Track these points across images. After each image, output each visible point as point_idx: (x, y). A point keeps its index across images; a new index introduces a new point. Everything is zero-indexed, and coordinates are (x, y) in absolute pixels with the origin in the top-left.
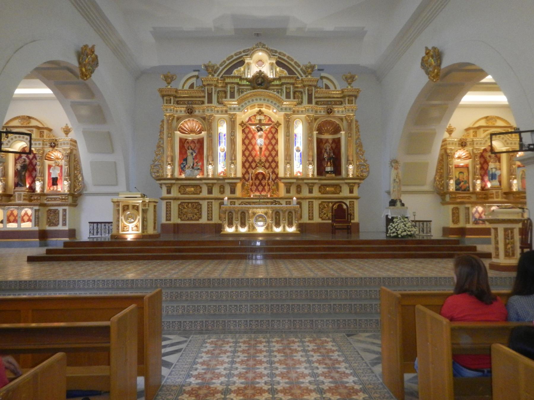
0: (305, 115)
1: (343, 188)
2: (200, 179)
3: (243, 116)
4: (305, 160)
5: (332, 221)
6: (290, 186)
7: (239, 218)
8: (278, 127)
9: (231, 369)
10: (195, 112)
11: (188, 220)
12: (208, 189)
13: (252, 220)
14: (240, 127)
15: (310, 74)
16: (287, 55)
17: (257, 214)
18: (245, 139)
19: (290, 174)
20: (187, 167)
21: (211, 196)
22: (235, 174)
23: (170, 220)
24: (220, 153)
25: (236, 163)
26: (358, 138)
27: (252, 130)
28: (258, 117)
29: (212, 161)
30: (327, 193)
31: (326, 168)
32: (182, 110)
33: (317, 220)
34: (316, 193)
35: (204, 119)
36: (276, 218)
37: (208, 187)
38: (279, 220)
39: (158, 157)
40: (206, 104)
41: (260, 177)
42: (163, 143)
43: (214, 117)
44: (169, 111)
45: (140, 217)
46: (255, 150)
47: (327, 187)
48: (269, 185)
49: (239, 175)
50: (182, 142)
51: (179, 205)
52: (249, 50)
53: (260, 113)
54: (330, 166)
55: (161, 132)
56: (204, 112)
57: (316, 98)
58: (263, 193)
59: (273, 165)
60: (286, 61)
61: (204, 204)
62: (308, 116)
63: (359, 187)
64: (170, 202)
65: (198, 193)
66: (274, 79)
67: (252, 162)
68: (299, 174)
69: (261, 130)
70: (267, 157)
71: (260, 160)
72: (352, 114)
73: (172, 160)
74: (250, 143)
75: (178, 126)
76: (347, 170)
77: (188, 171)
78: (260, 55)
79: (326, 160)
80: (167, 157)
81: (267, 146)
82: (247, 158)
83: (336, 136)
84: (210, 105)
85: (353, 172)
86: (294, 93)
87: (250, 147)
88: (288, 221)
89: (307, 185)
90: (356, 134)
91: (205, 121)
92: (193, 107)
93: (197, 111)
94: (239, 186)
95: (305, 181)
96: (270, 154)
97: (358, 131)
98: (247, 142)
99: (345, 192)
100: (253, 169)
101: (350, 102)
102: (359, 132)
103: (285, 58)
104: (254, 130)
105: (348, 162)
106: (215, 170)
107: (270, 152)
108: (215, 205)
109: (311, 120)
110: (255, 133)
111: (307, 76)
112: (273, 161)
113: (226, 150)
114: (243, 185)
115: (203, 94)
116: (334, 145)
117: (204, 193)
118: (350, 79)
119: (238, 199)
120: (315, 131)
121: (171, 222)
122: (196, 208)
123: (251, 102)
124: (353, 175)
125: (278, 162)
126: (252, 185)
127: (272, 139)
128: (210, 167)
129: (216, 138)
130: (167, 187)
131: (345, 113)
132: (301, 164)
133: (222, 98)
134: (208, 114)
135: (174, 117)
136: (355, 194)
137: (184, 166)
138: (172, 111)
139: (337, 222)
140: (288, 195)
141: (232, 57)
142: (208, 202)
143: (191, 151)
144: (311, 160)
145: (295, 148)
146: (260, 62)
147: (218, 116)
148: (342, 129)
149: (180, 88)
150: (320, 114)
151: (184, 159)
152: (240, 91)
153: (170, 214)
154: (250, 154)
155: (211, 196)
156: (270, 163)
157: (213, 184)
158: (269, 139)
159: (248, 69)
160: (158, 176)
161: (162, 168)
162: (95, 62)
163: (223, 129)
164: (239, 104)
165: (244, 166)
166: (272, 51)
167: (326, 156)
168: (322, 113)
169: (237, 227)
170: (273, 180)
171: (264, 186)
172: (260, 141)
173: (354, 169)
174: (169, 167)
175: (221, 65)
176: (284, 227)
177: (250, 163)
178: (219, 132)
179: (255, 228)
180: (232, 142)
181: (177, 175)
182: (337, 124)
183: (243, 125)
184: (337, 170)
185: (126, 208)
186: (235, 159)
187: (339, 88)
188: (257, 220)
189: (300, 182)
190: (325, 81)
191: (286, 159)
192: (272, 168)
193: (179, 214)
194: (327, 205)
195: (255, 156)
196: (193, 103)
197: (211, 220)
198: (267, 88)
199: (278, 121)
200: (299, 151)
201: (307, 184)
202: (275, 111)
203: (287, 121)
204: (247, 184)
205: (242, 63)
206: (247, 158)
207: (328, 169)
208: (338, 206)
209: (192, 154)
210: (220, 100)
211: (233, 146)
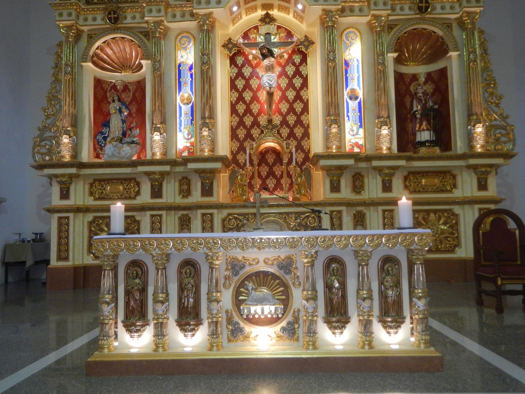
0: (369, 18)
1: (459, 179)
2: (133, 164)
6: (340, 176)
7: (173, 289)
8: (307, 48)
10: (125, 18)
12: (152, 185)
14: (227, 52)
17: (248, 270)
18: (236, 78)
19: (339, 148)
20: (109, 139)
22: (212, 150)
23: (66, 259)
24: (180, 108)
25: (214, 125)
26: (486, 69)
27: (251, 57)
28: (264, 29)
29: (161, 123)
30: (425, 190)
31: (418, 134)
35: (147, 34)
36: (329, 287)
37: (152, 181)
38: (344, 297)
39: (49, 121)
41: (271, 158)
43: (167, 29)
44: (65, 17)
46: (259, 102)
47: (423, 176)
48: (289, 176)
51: (90, 223)
53: (267, 20)
54: (428, 130)
55: (56, 67)
59: (299, 132)
62: (376, 17)
63: (496, 174)
64: (68, 218)
65: (132, 196)
67: (252, 126)
68: (356, 150)
69: (271, 54)
70: (284, 117)
71: (270, 121)
72: (478, 10)
73: (75, 123)
74: (247, 86)
75: (89, 50)
76: (470, 138)
77: (109, 149)
79: (418, 116)
82: (241, 118)
87: (248, 96)
88: (383, 296)
89: (377, 171)
90: (481, 60)
91: (148, 40)
92: (119, 8)
93: (129, 17)
94: (224, 177)
95: (375, 163)
96: (291, 110)
98: (240, 84)
102: (486, 54)
104: (255, 57)
107: (291, 104)
109: (380, 26)
110: (258, 65)
112: (299, 122)
113: (193, 99)
114: (232, 178)
116: (429, 88)
119: (220, 207)
120: (391, 52)
121: (69, 263)
124: (482, 147)
125: (308, 125)
126: (252, 178)
127: (294, 76)
128: (157, 137)
130: (61, 183)
131: (457, 9)
132: (361, 126)
137: (105, 138)
138: (73, 17)
140: (335, 196)
142: (152, 216)
143: (117, 105)
144: (386, 116)
148: (451, 46)
150: (401, 13)
153: (67, 244)
154: (248, 111)
156: (292, 129)
157: (163, 174)
158: (287, 76)
165: (234, 135)
167: (417, 107)
168: (407, 11)
174: (65, 140)
177: (249, 130)
178: (178, 62)
179: (241, 330)
182: (438, 37)
183: (230, 46)
186: (212, 116)
189: (363, 165)
191: (329, 115)
192: (296, 138)
194: (424, 219)
195: (259, 114)
199: (306, 36)
200: (356, 98)
201: (379, 170)
202: (300, 7)
203: (328, 27)
204: (242, 175)
206: (241, 118)
209: (120, 111)
211: (207, 87)
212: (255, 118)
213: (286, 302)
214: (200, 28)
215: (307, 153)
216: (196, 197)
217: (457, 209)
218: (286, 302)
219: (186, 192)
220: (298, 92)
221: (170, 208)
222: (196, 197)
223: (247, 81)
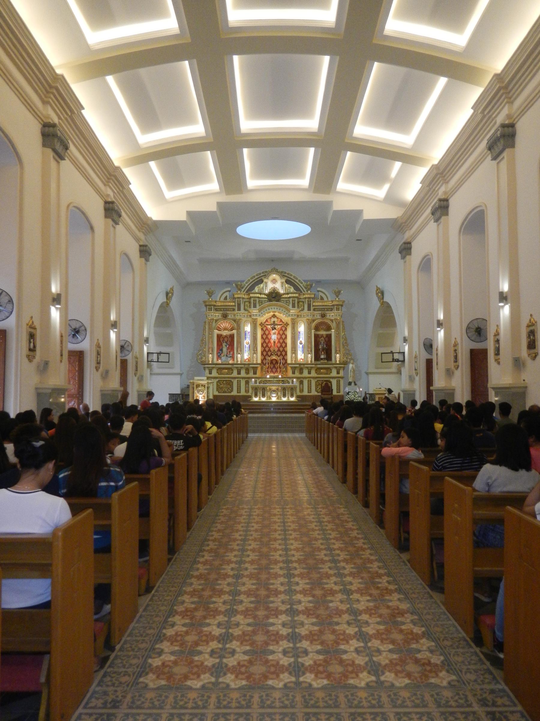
2: (232, 364)
3: (262, 319)
5: (322, 394)
9: (247, 527)
11: (224, 392)
12: (238, 371)
13: (269, 393)
15: (309, 289)
16: (293, 275)
19: (295, 361)
20: (222, 355)
21: (239, 376)
22: (256, 361)
28: (273, 319)
30: (322, 374)
32: (218, 315)
33: (314, 393)
34: (313, 374)
40: (237, 312)
41: (274, 362)
42: (205, 338)
45: (206, 391)
48: (280, 368)
49: (259, 361)
50: (219, 336)
51: (217, 382)
52: (266, 272)
56: (234, 315)
57: (313, 306)
58: (276, 375)
59: (283, 353)
60: (293, 280)
61: (235, 382)
62: (308, 319)
63: (344, 369)
66: (284, 294)
69: (275, 329)
74: (267, 338)
76: (335, 357)
77: (224, 358)
78: (274, 276)
81: (279, 340)
84: (239, 312)
85: (340, 358)
86: (298, 302)
87: (267, 341)
93: (230, 315)
95: (306, 366)
96: (281, 346)
97: (344, 329)
98: (264, 337)
99: (334, 373)
100: (269, 357)
101: (338, 309)
103: (292, 277)
105: (336, 353)
106: (242, 357)
111: (307, 291)
112: (284, 350)
114: (262, 368)
115: (233, 304)
116: (327, 339)
117: (235, 374)
118: (338, 294)
119: (258, 378)
122: (229, 384)
123: (268, 311)
128: (239, 356)
129: (243, 335)
133: (247, 306)
134: (238, 318)
135: (213, 319)
139: (324, 394)
140: (293, 375)
141: (254, 277)
143: (225, 344)
145: (299, 342)
146: (274, 281)
147: (244, 319)
149: (218, 300)
152: (261, 303)
154: (267, 346)
155: (239, 376)
157: (241, 368)
159: (266, 286)
161: (204, 356)
162: (173, 294)
163: (248, 328)
164: (260, 311)
165: (262, 354)
166: (282, 272)
168: (318, 317)
169: (260, 397)
170: (283, 364)
171: (277, 369)
172: (274, 337)
173: (340, 357)
174: (210, 356)
175: (246, 283)
176: (288, 397)
181: (215, 361)
184: (329, 357)
185: (198, 386)
186: (257, 350)
187: (330, 299)
188: (271, 393)
189: (302, 366)
190: (321, 294)
191: (292, 350)
193: (217, 389)
196: (227, 310)
197: (240, 392)
198: (278, 301)
201: (307, 367)
205: (261, 281)
207: (322, 357)
208: (326, 384)
209: (226, 346)
210: (246, 308)
212: (269, 348)
213: (277, 394)
214: (253, 322)
215: (286, 360)
216: (251, 374)
217: (331, 380)
218: (277, 394)
219: (247, 372)
220: (284, 340)
221: (243, 378)
222: (251, 374)
223: (267, 336)
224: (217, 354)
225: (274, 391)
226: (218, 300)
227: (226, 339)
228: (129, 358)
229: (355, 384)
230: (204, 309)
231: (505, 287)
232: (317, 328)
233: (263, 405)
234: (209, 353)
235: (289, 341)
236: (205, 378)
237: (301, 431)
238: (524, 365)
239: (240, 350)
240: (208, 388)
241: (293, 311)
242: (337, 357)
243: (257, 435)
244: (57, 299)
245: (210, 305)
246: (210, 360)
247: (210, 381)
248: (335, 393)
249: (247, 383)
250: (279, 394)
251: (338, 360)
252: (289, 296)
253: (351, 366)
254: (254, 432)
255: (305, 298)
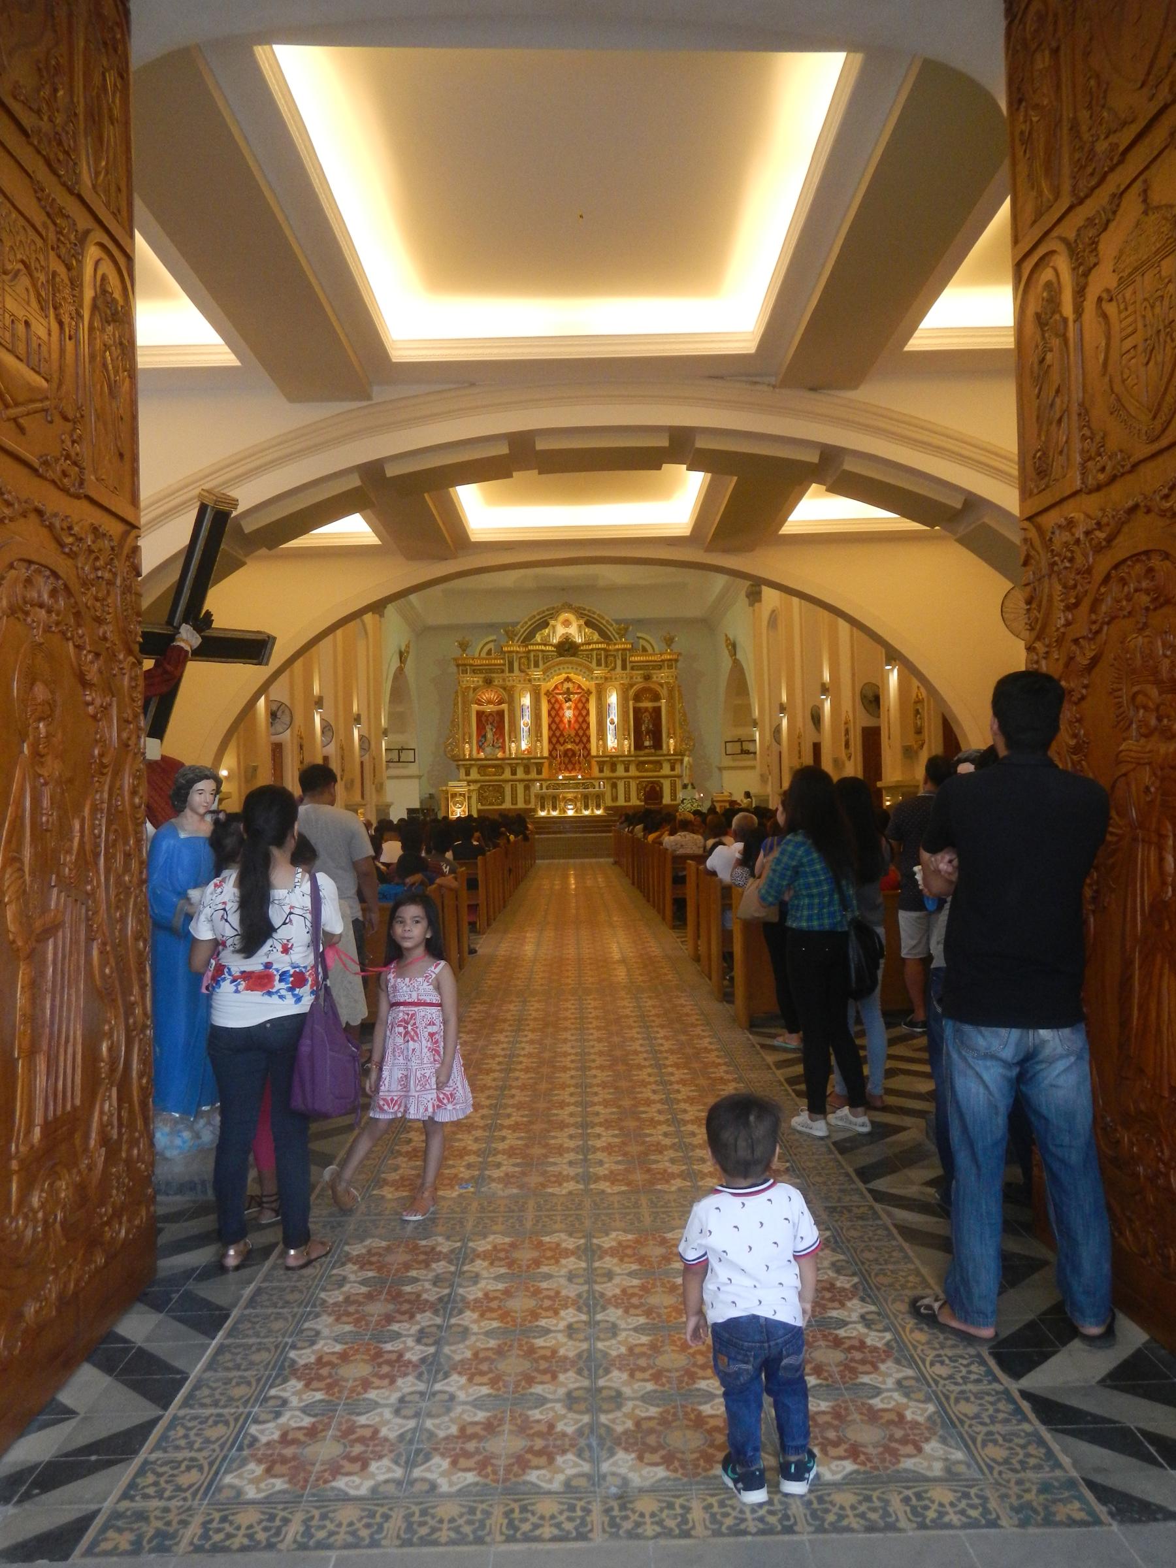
3: (550, 685)
4: (621, 733)
28: (566, 685)
30: (646, 771)
32: (476, 680)
33: (635, 801)
34: (633, 771)
41: (570, 754)
45: (466, 803)
49: (546, 754)
50: (480, 714)
51: (479, 790)
56: (504, 680)
58: (573, 774)
59: (585, 740)
73: (470, 738)
74: (557, 714)
76: (668, 746)
77: (488, 750)
80: (464, 735)
83: (656, 704)
86: (606, 657)
87: (557, 720)
96: (581, 728)
98: (553, 713)
99: (666, 770)
101: (670, 667)
106: (518, 747)
108: (520, 788)
112: (585, 734)
114: (550, 764)
117: (507, 775)
118: (669, 641)
128: (513, 745)
129: (518, 713)
134: (509, 684)
136: (677, 771)
146: (567, 623)
151: (482, 735)
152: (546, 659)
154: (558, 728)
156: (581, 738)
160: (453, 756)
161: (457, 746)
163: (526, 701)
164: (545, 671)
165: (550, 741)
168: (640, 680)
172: (569, 714)
174: (467, 746)
180: (537, 717)
184: (658, 744)
187: (657, 651)
196: (491, 671)
198: (574, 655)
201: (623, 762)
205: (547, 625)
207: (647, 743)
215: (589, 751)
216: (533, 775)
217: (662, 780)
219: (527, 772)
222: (533, 775)
224: (478, 742)
225: (570, 800)
226: (477, 655)
227: (491, 719)
228: (366, 758)
229: (694, 788)
230: (453, 669)
231: (826, 677)
232: (637, 698)
233: (554, 823)
234: (464, 742)
235: (593, 719)
236: (465, 783)
237: (609, 856)
238: (844, 765)
239: (515, 734)
240: (469, 798)
241: (597, 672)
242: (671, 744)
243: (547, 861)
244: (319, 703)
245: (465, 665)
246: (467, 753)
247: (472, 788)
248: (667, 800)
249: (527, 788)
250: (579, 804)
251: (672, 748)
252: (591, 647)
253: (686, 759)
254: (543, 858)
255: (618, 650)
